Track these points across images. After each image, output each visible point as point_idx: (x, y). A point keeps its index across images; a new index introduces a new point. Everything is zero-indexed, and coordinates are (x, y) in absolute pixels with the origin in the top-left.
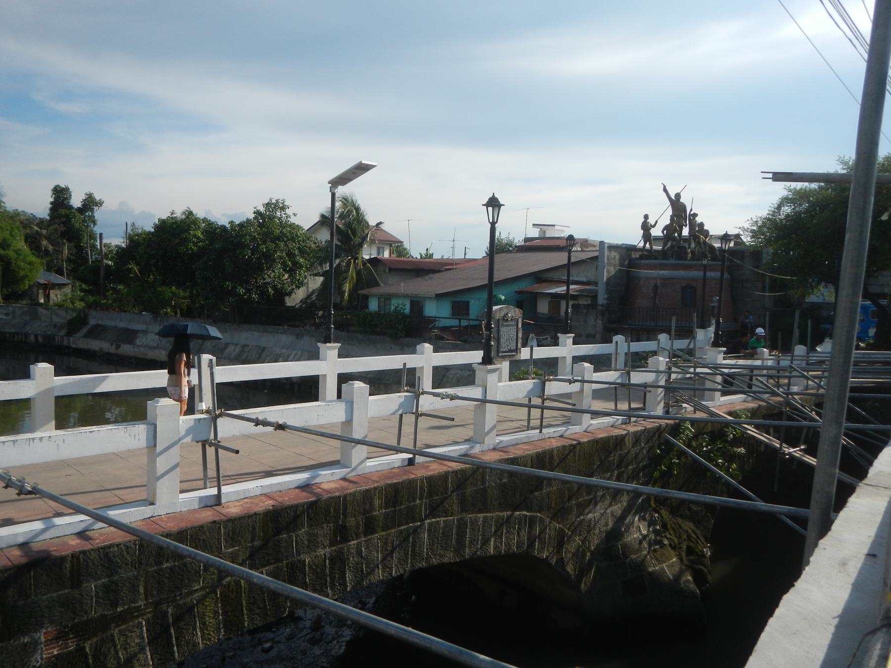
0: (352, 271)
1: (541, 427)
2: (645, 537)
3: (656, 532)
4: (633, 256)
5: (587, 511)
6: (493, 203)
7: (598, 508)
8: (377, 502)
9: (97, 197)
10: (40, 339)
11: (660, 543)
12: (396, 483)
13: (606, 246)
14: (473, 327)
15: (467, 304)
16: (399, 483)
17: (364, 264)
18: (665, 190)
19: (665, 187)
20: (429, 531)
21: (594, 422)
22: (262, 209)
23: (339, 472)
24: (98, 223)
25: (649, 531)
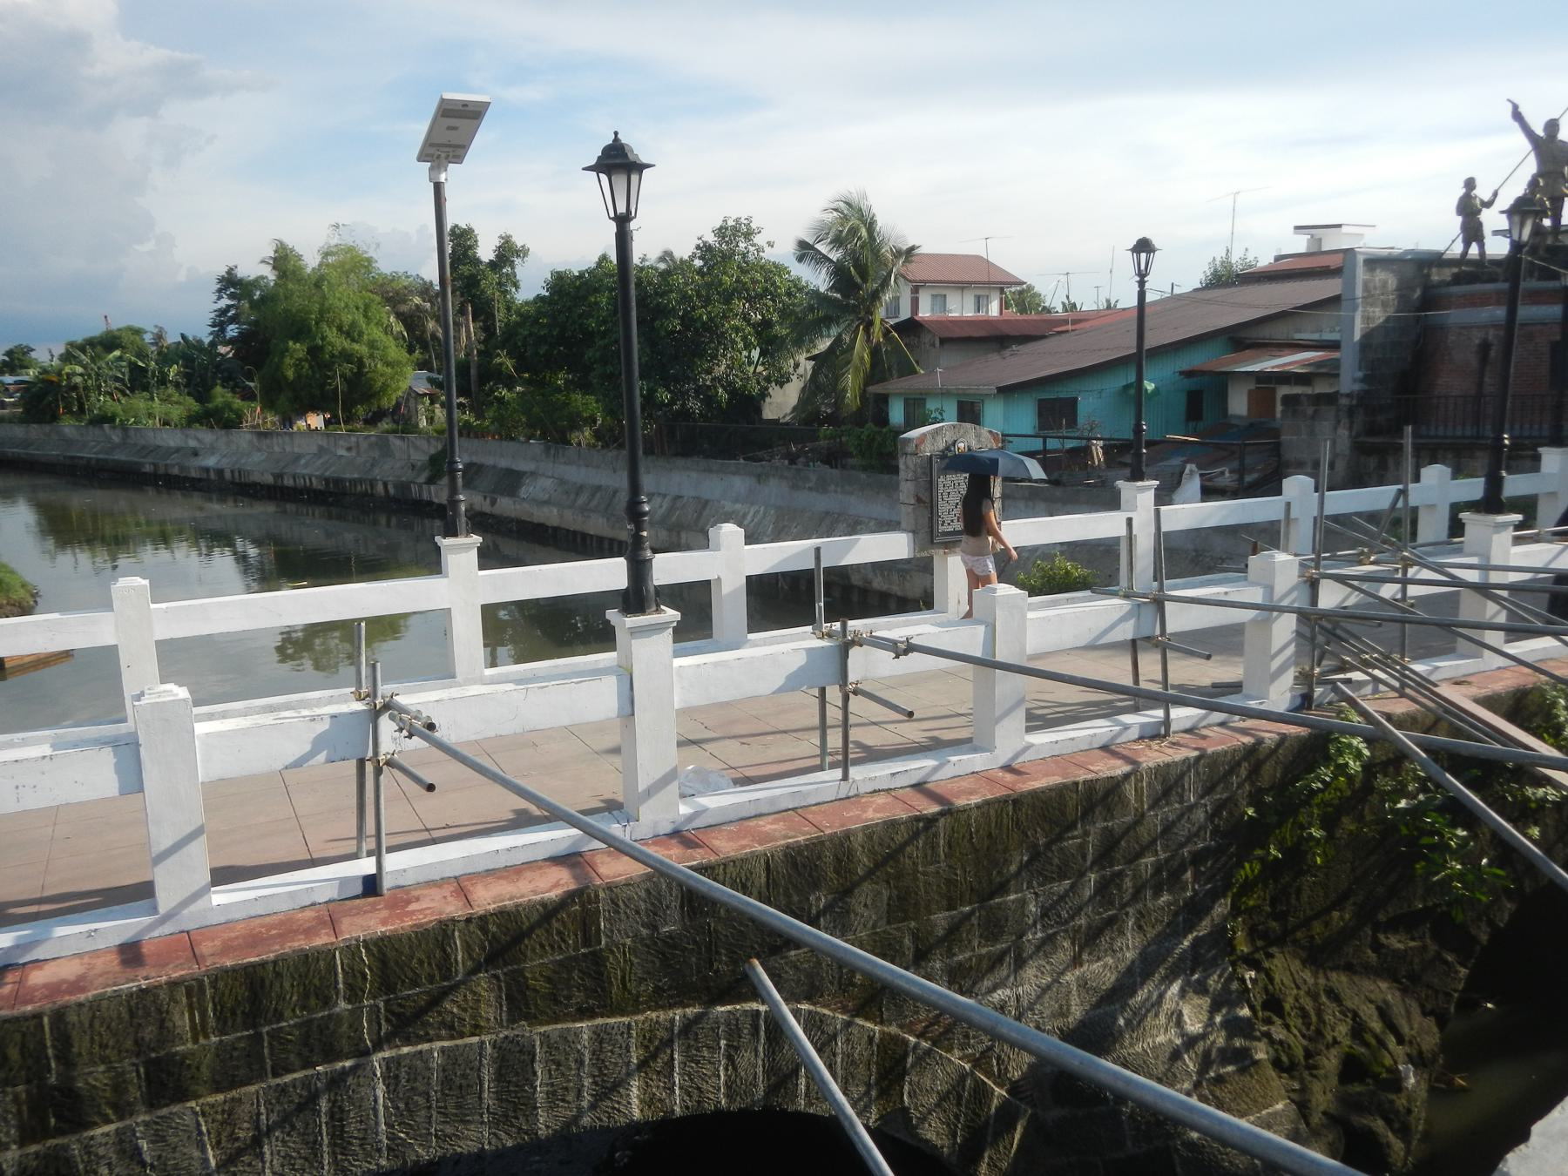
0: (861, 350)
1: (845, 764)
2: (1191, 1041)
3: (1235, 1027)
4: (1435, 278)
5: (987, 983)
6: (617, 162)
7: (1029, 972)
8: (182, 1021)
9: (519, 241)
10: (392, 490)
11: (1241, 1058)
12: (253, 965)
13: (1361, 259)
14: (1073, 452)
15: (1074, 401)
16: (263, 964)
17: (886, 333)
18: (1517, 116)
19: (1515, 107)
20: (391, 1080)
21: (1041, 738)
22: (711, 239)
23: (114, 928)
24: (522, 284)
25: (1210, 1023)
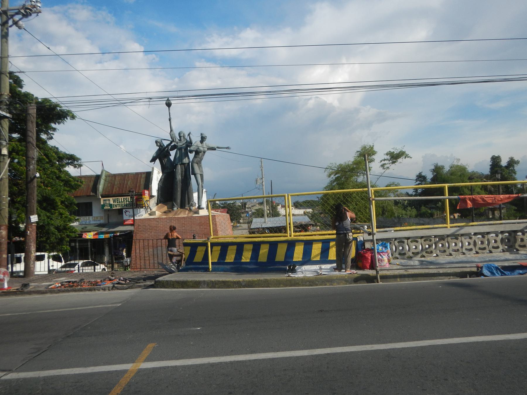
9: (516, 159)
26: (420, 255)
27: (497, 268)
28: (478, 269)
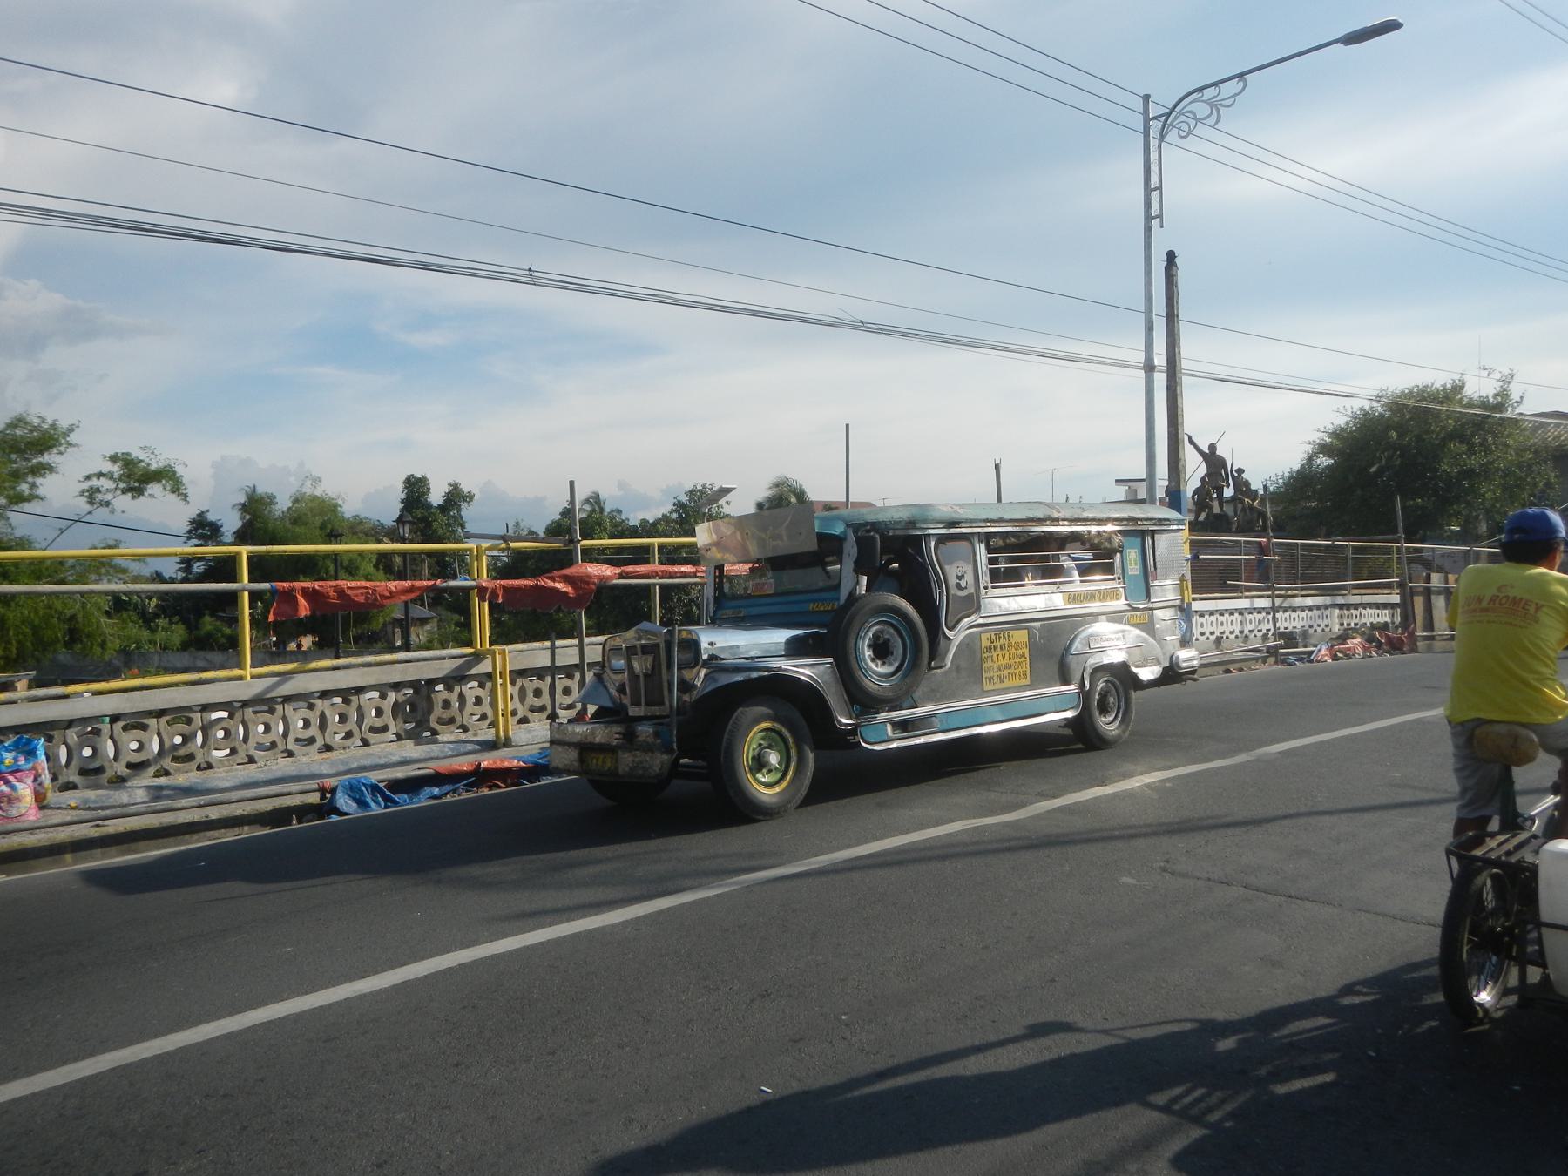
9: (465, 488)
22: (684, 499)
26: (151, 770)
27: (374, 789)
28: (323, 797)
